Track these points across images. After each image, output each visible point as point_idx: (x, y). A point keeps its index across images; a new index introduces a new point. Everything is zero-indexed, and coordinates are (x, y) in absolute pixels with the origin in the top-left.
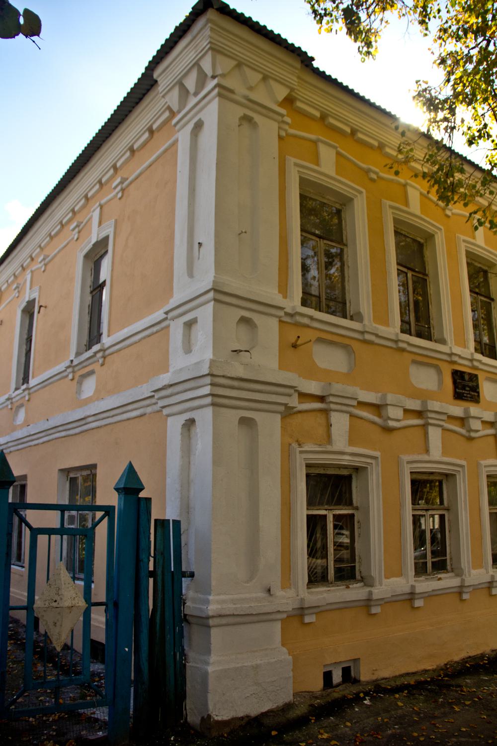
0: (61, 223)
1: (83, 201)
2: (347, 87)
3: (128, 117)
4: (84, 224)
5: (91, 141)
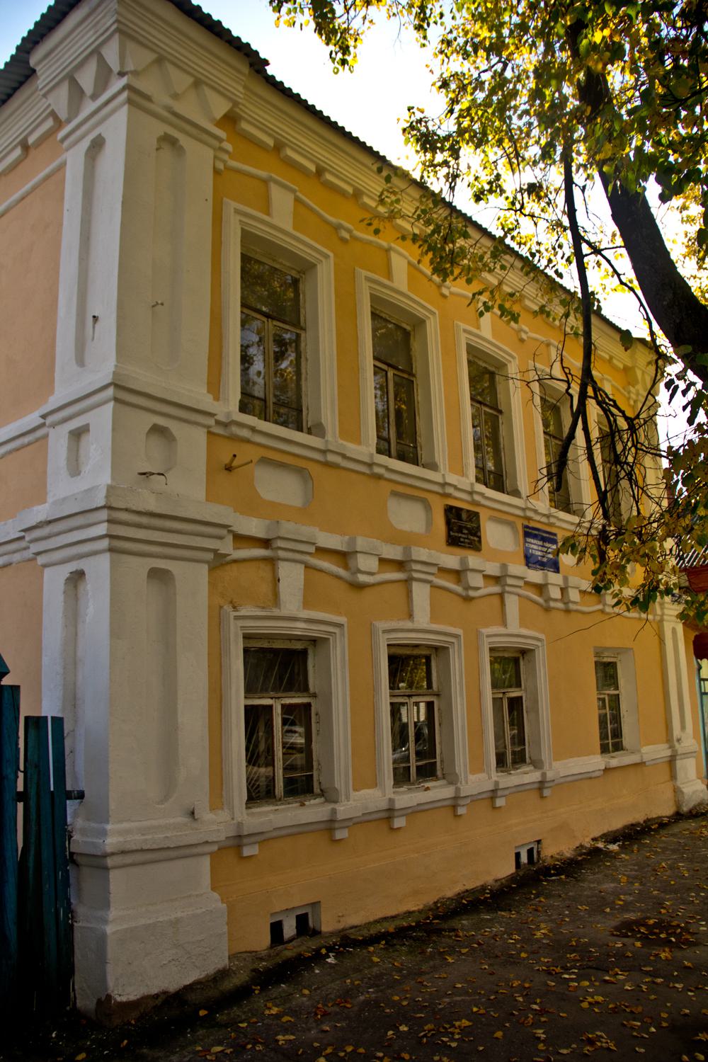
2: (371, 148)
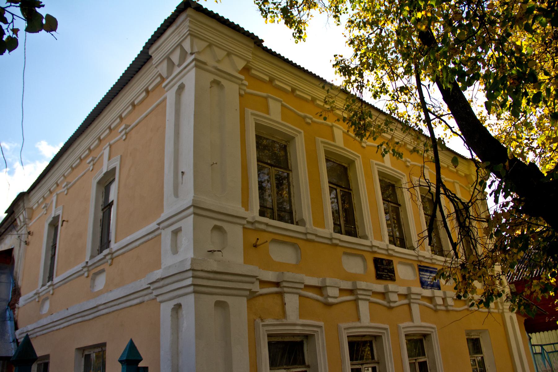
0: (71, 167)
1: (70, 170)
3: (123, 89)
4: (71, 184)
5: (86, 119)
